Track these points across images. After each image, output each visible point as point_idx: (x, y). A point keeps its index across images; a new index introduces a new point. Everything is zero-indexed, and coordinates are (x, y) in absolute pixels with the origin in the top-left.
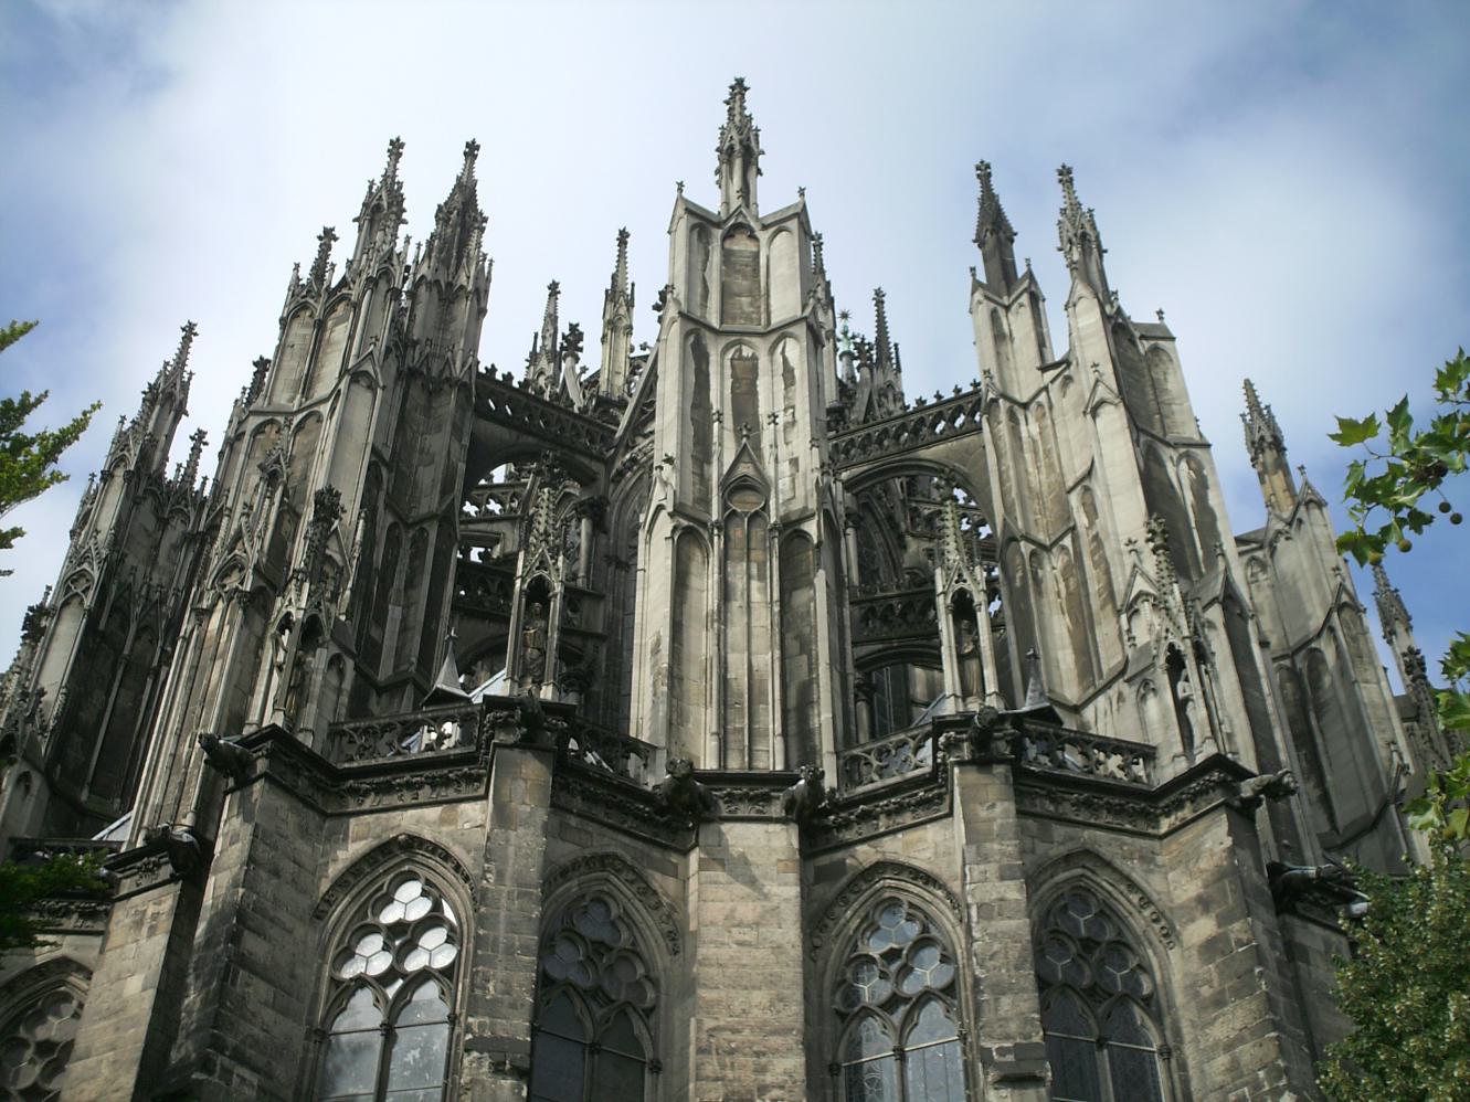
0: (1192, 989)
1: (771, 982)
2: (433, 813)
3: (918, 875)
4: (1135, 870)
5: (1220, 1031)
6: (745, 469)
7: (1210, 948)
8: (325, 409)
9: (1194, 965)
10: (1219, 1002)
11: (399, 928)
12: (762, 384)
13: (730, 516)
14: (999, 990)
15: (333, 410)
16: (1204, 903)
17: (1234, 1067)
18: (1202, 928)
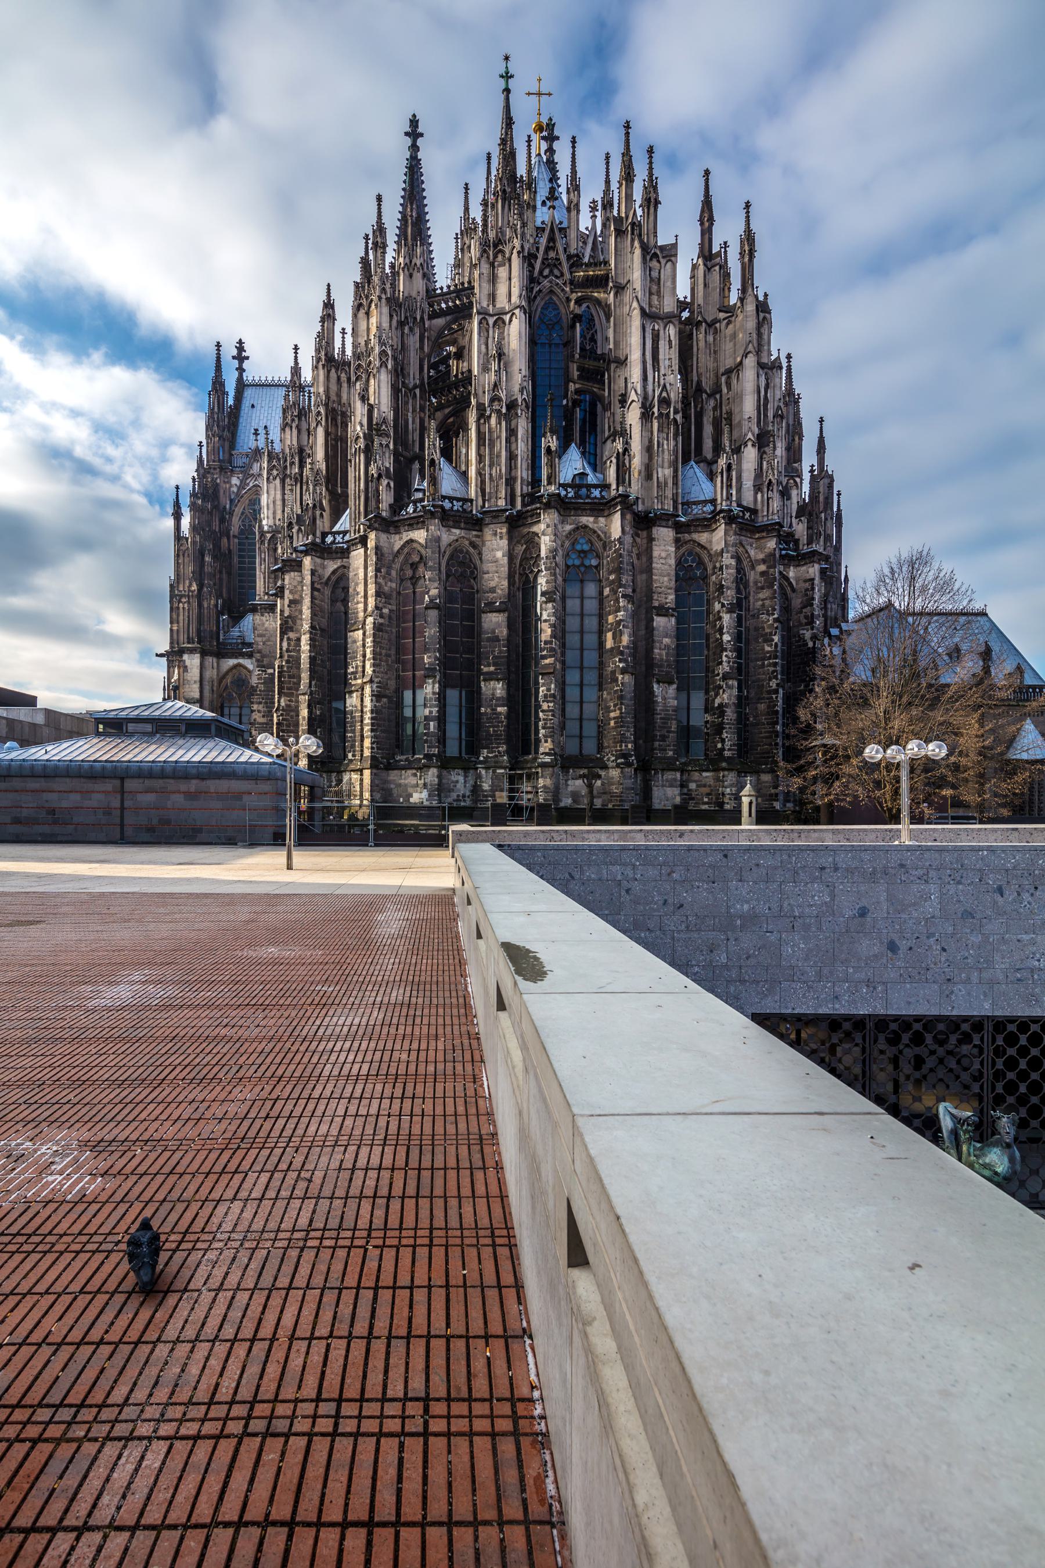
0: (756, 583)
1: (669, 575)
2: (591, 519)
3: (699, 544)
4: (748, 548)
5: (761, 596)
6: (664, 394)
7: (763, 574)
8: (507, 318)
9: (758, 577)
10: (762, 588)
11: (583, 551)
12: (661, 343)
13: (661, 415)
14: (728, 588)
15: (511, 321)
16: (764, 561)
17: (763, 605)
18: (762, 568)
